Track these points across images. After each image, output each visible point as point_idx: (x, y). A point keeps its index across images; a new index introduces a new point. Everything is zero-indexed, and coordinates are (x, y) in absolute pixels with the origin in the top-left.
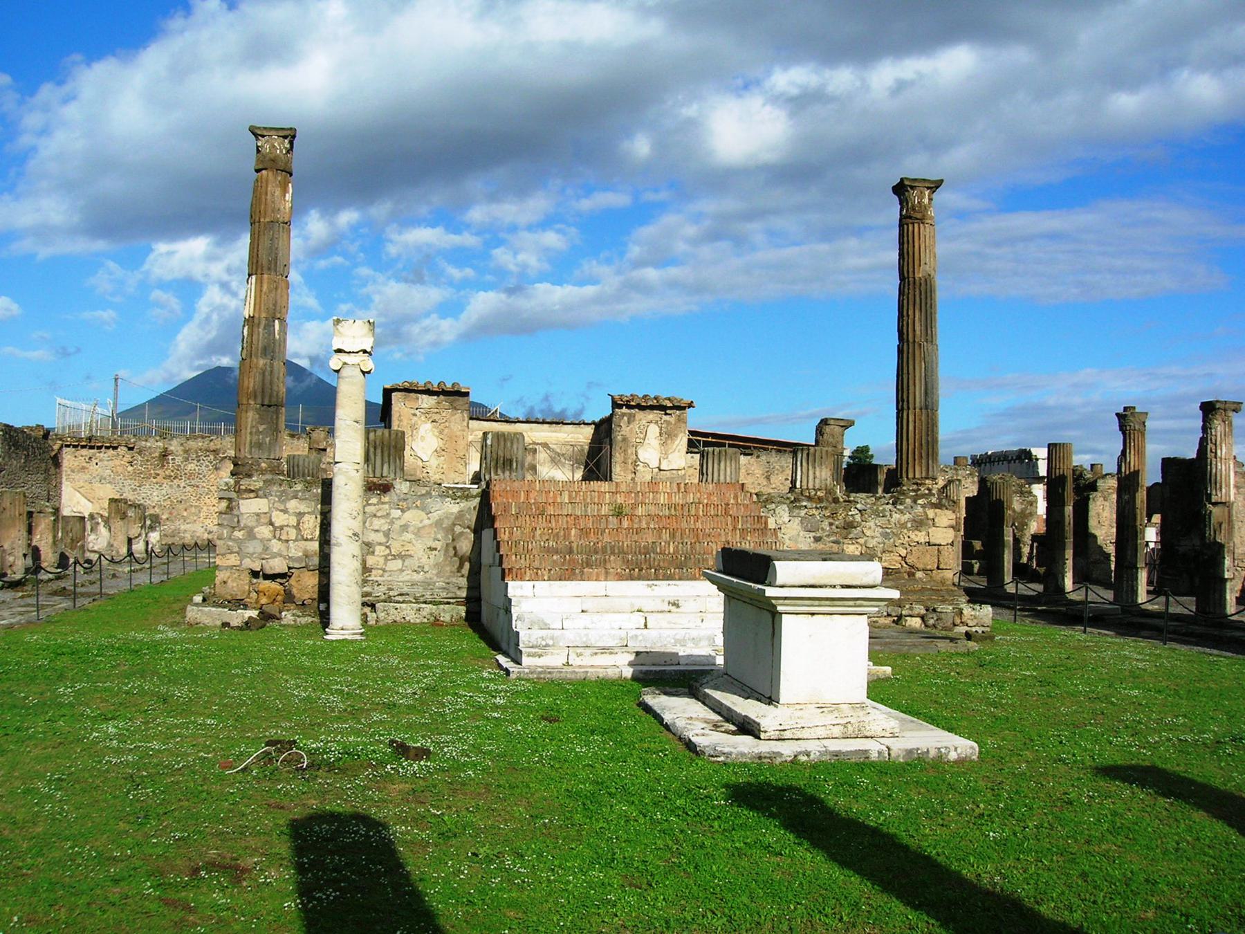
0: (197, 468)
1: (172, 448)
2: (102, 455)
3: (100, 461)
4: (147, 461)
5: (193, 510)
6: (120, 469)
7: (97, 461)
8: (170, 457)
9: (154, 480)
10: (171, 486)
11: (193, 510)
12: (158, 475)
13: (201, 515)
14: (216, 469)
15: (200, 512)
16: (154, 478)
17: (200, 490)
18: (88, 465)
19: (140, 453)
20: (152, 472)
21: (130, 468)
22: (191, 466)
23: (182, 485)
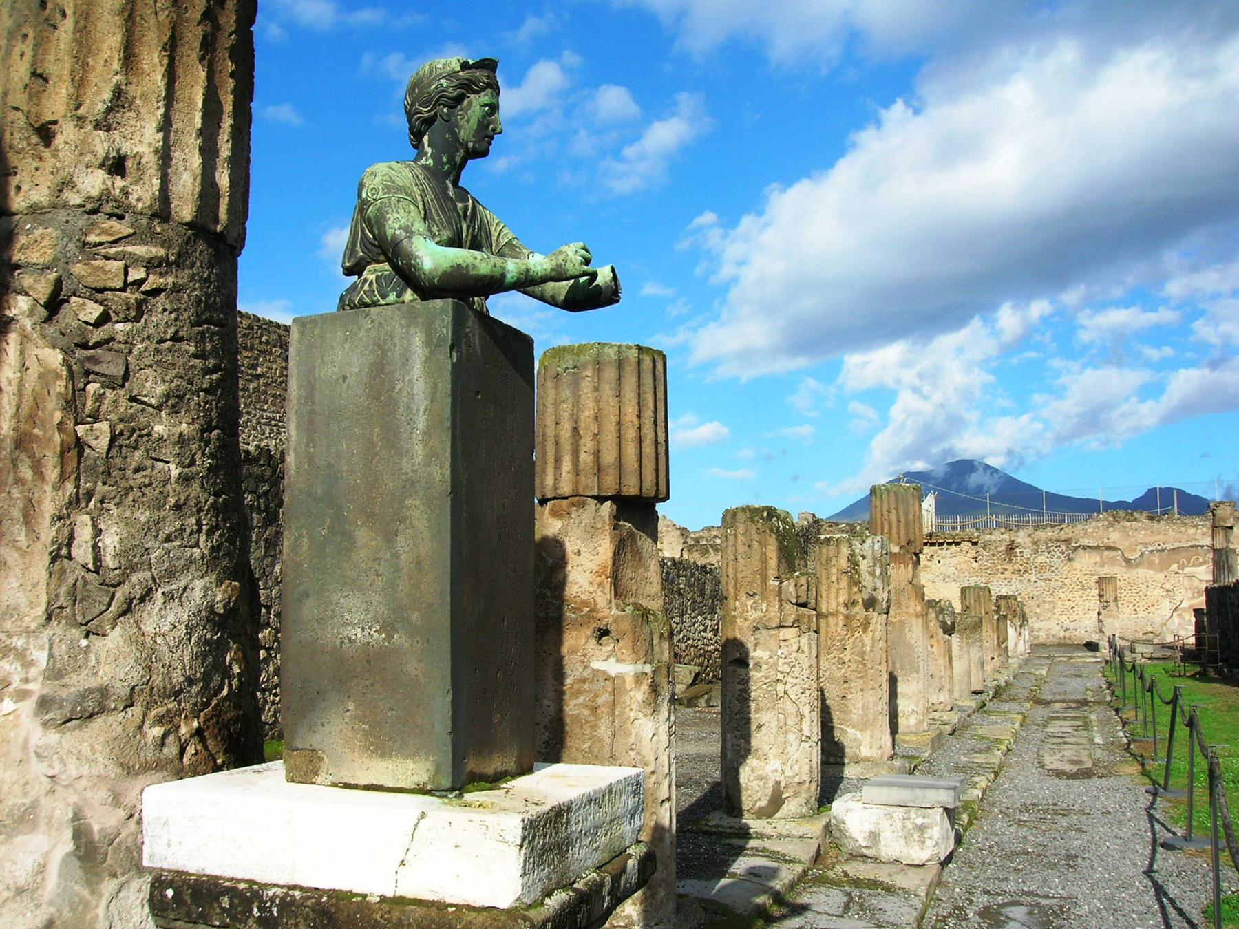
0: (1048, 561)
1: (1019, 540)
2: (944, 552)
3: (943, 558)
4: (993, 555)
5: (1047, 606)
6: (964, 566)
7: (939, 558)
8: (1018, 550)
9: (1003, 576)
10: (1021, 581)
11: (1047, 606)
12: (1006, 570)
13: (1056, 611)
14: (1070, 560)
15: (1054, 608)
16: (1002, 573)
17: (1053, 584)
18: (930, 563)
19: (984, 548)
20: (999, 567)
21: (975, 565)
22: (1041, 559)
23: (1033, 579)
